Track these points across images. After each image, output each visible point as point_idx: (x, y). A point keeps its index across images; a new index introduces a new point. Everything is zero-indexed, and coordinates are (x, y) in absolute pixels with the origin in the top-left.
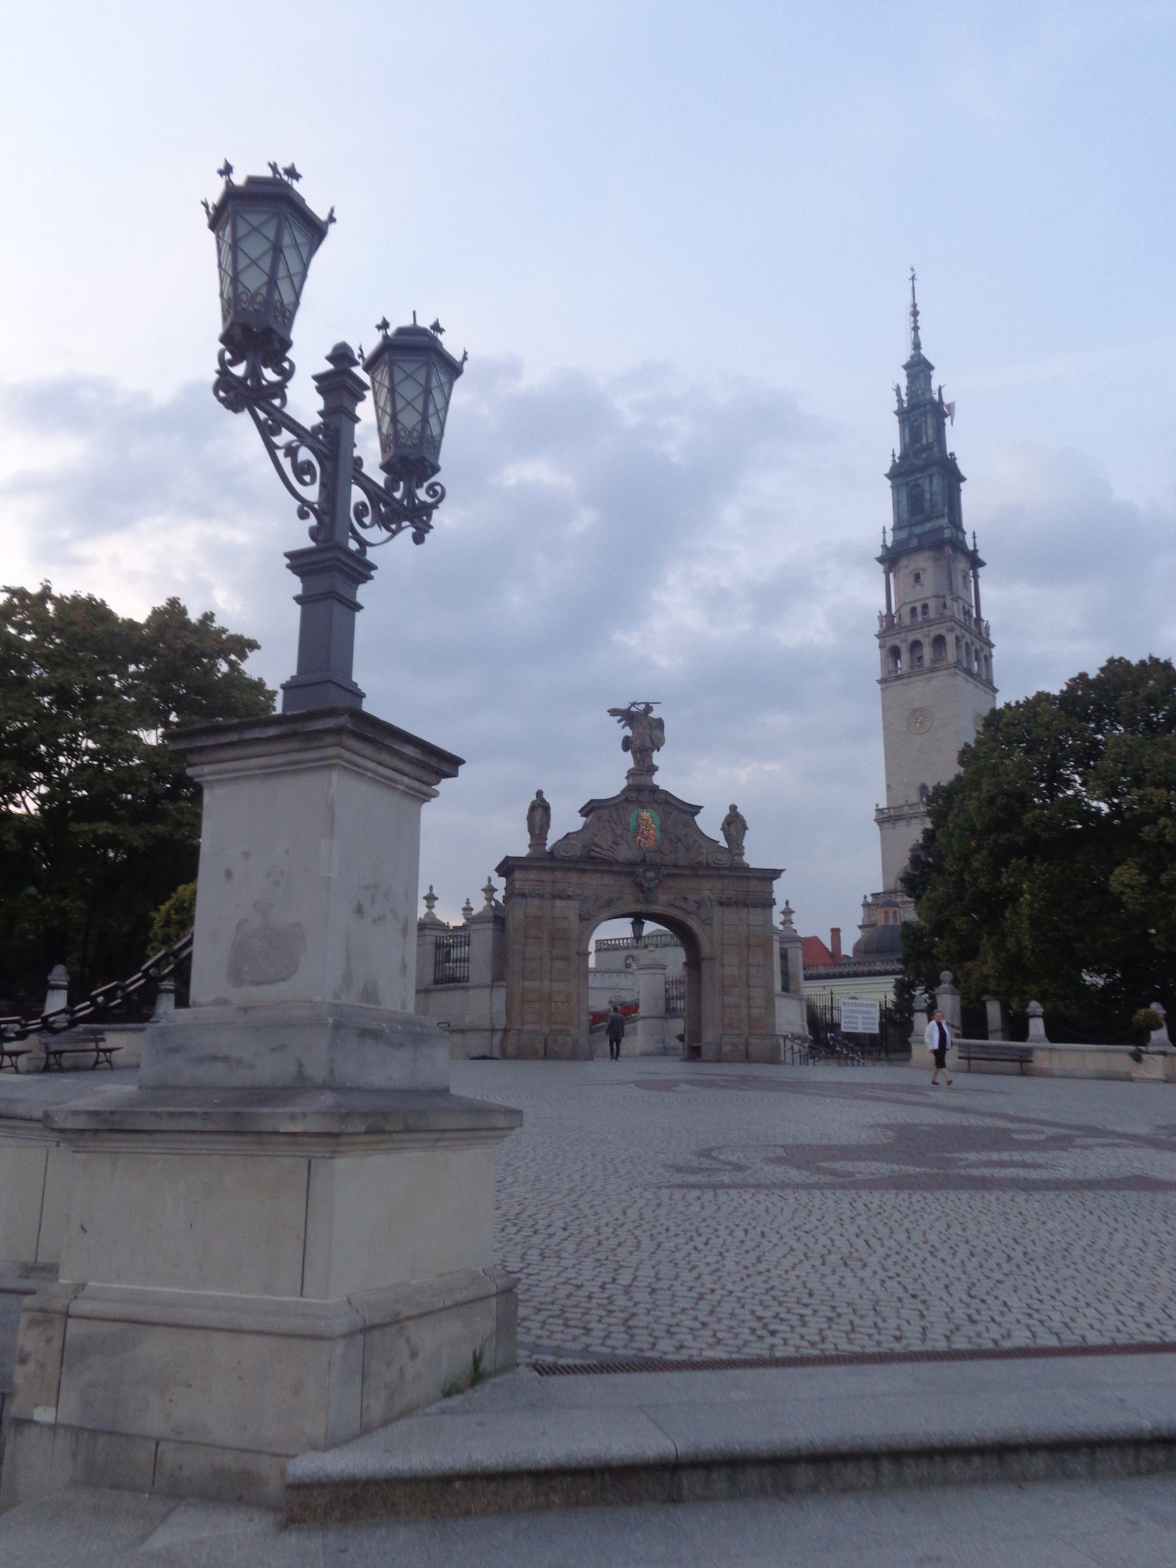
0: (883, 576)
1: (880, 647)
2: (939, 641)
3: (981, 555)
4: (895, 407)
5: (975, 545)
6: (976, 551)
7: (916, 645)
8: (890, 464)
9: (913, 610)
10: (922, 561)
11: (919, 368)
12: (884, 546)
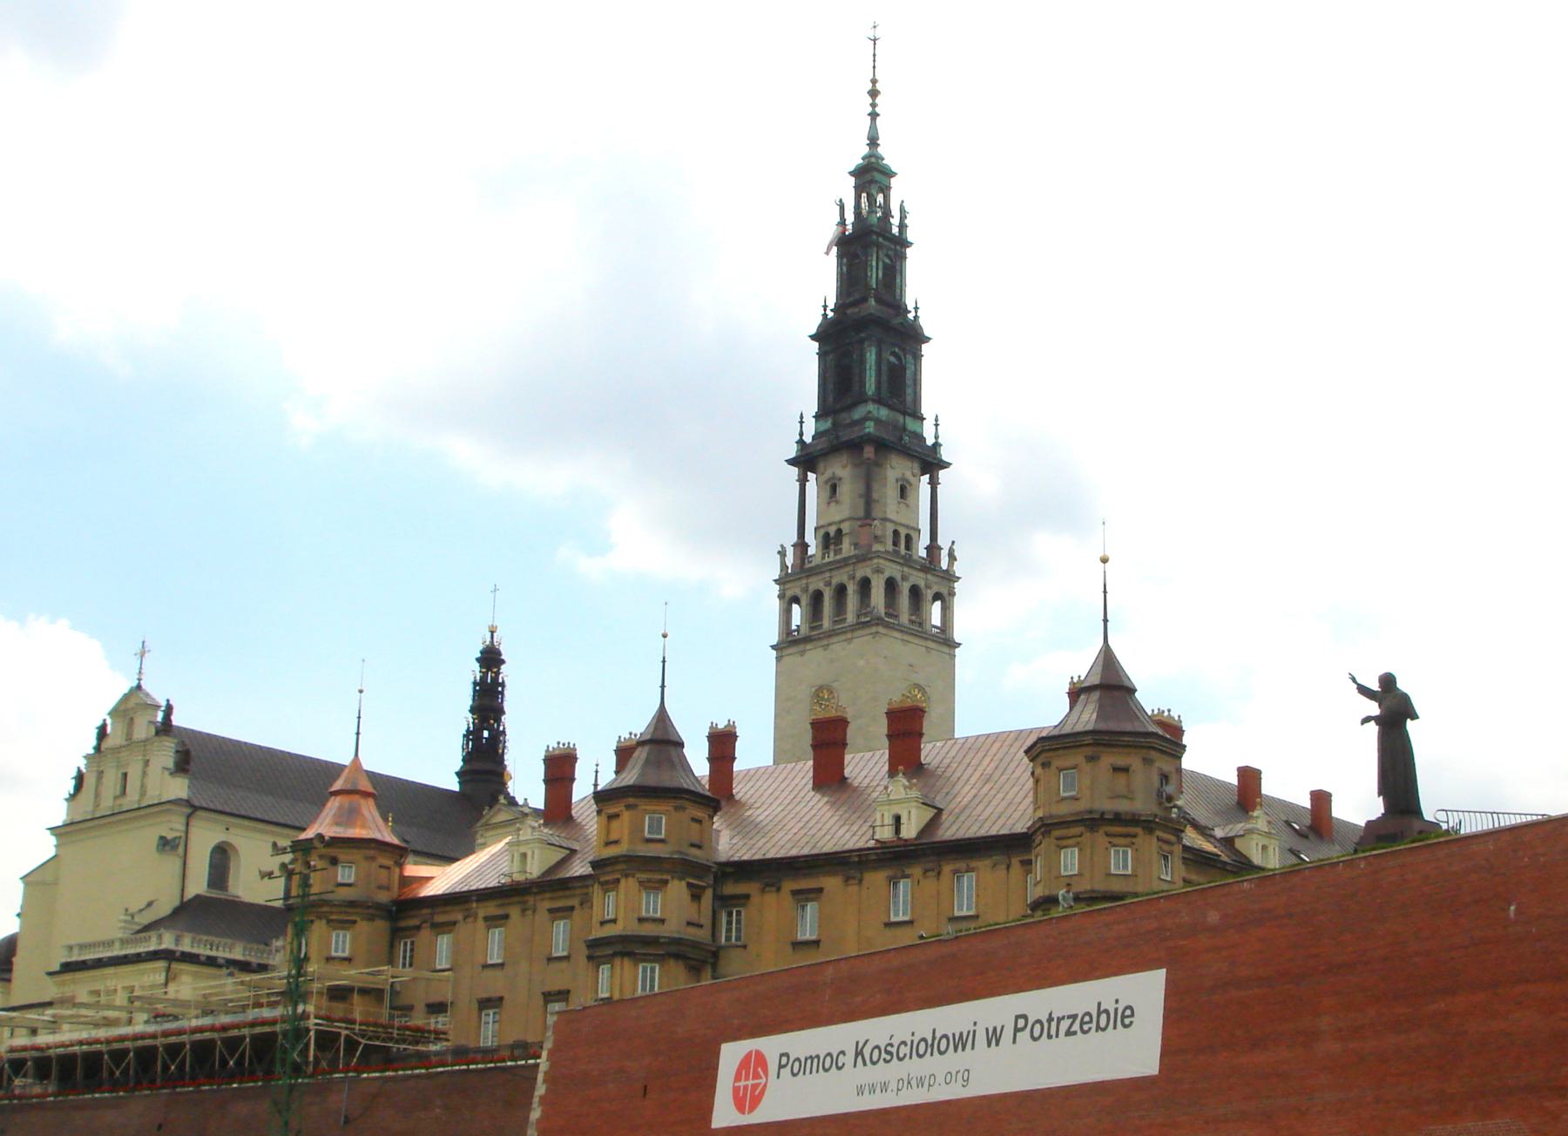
3: (945, 455)
5: (936, 437)
6: (936, 445)
8: (819, 319)
9: (827, 535)
10: (841, 468)
11: (872, 176)
12: (801, 442)
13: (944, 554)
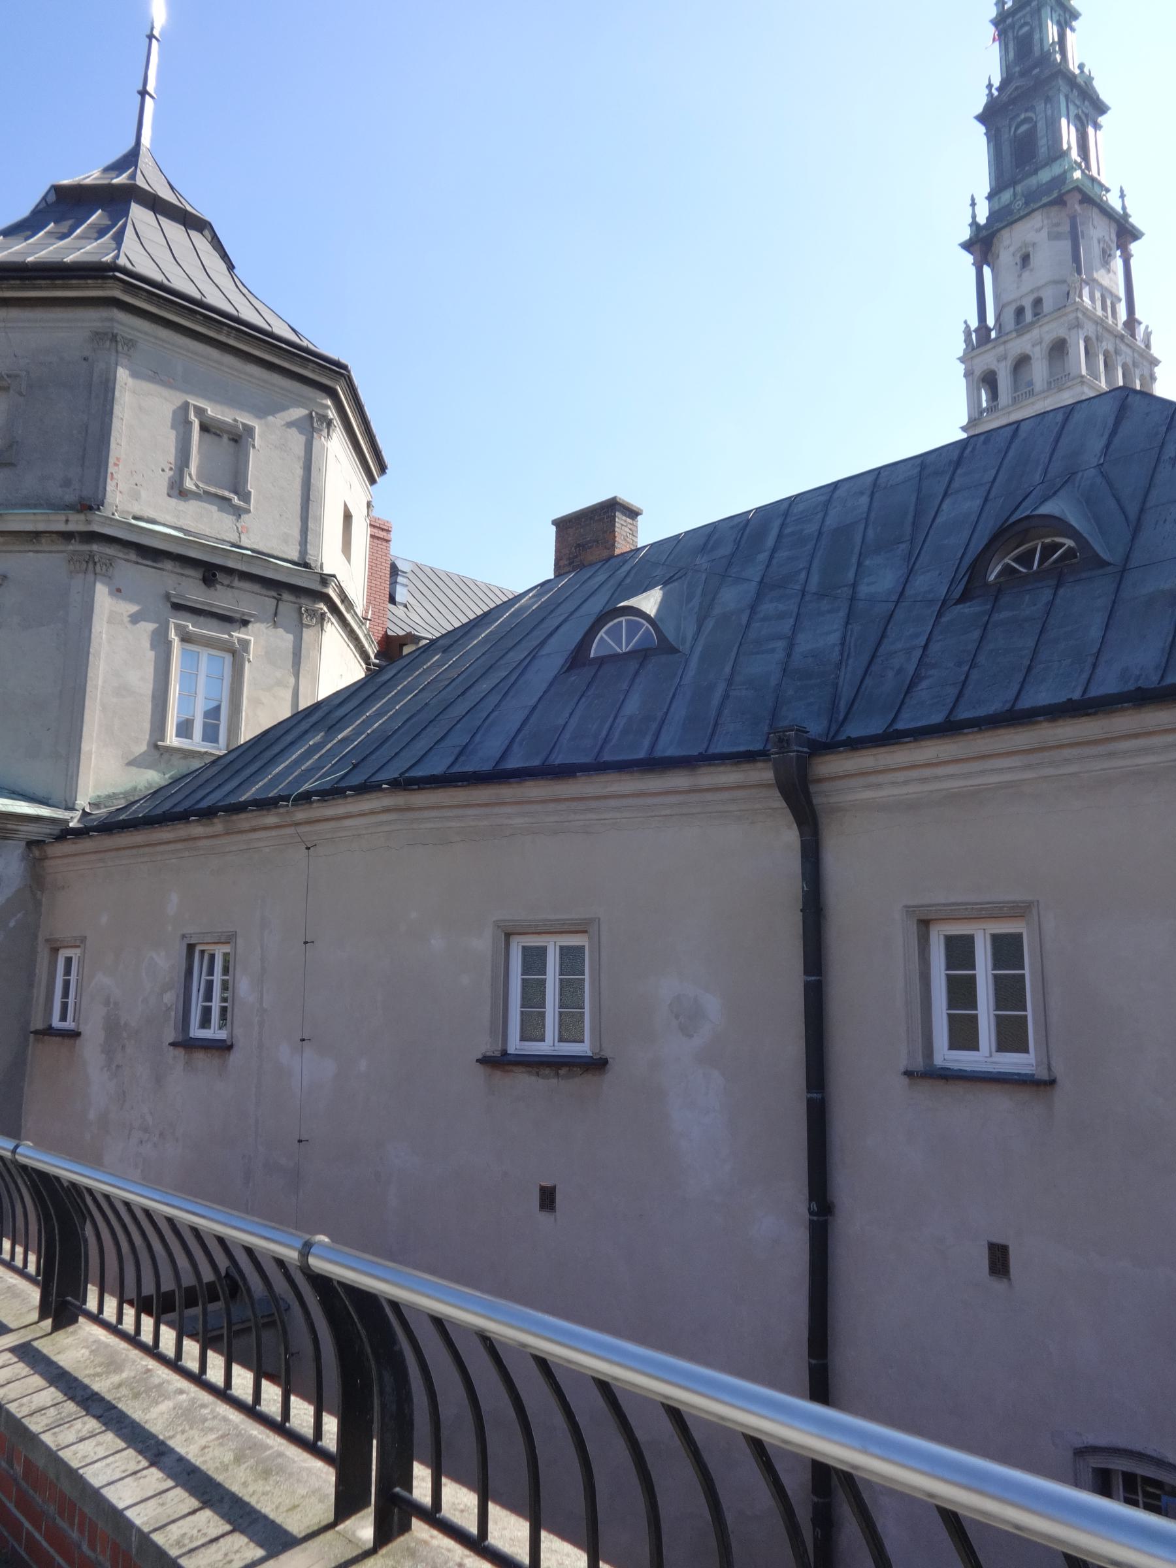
0: (973, 271)
1: (965, 375)
2: (1059, 349)
4: (993, 12)
5: (1124, 208)
6: (1126, 215)
7: (1022, 362)
9: (1020, 312)
12: (974, 224)
13: (1142, 327)
